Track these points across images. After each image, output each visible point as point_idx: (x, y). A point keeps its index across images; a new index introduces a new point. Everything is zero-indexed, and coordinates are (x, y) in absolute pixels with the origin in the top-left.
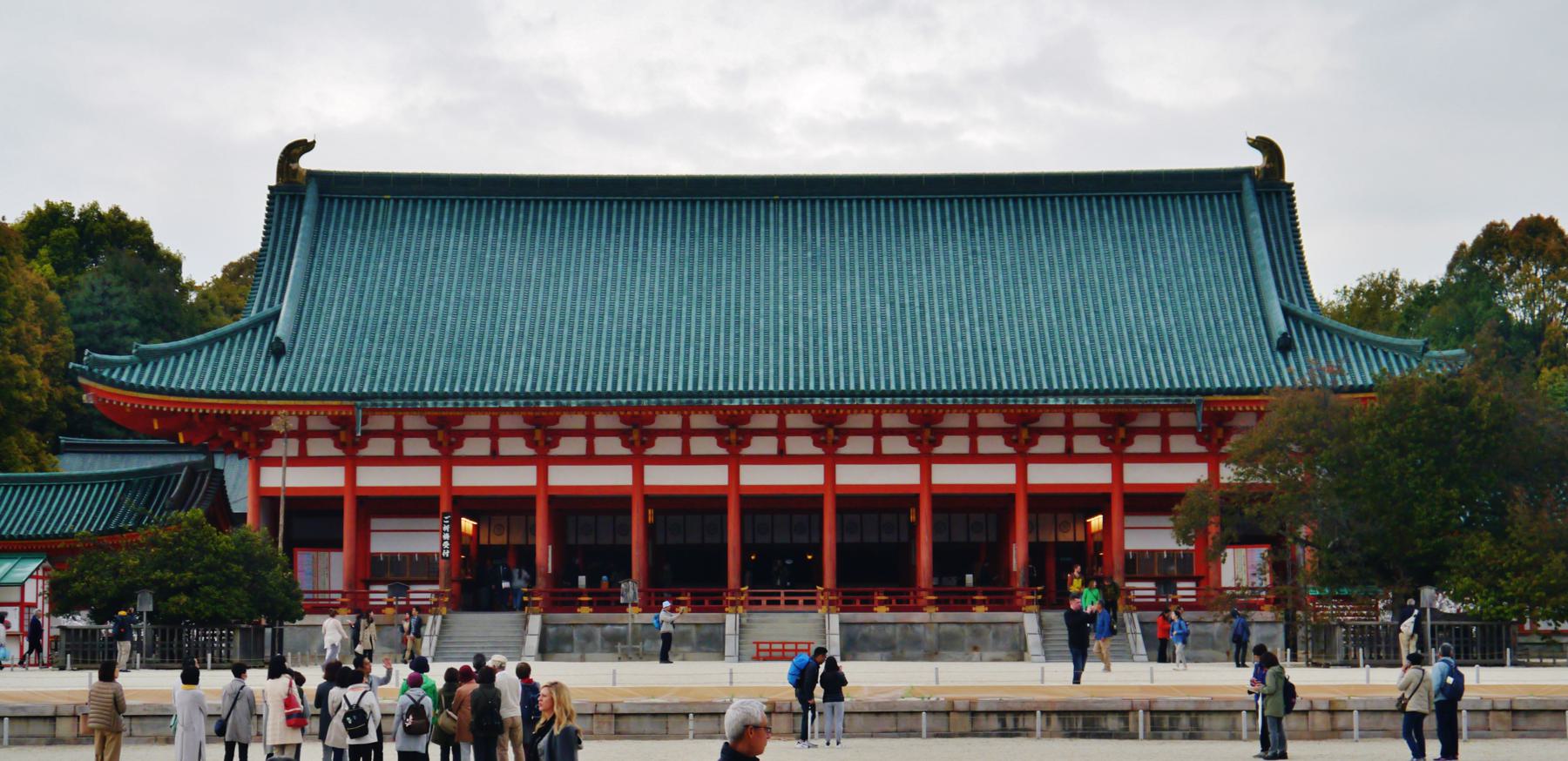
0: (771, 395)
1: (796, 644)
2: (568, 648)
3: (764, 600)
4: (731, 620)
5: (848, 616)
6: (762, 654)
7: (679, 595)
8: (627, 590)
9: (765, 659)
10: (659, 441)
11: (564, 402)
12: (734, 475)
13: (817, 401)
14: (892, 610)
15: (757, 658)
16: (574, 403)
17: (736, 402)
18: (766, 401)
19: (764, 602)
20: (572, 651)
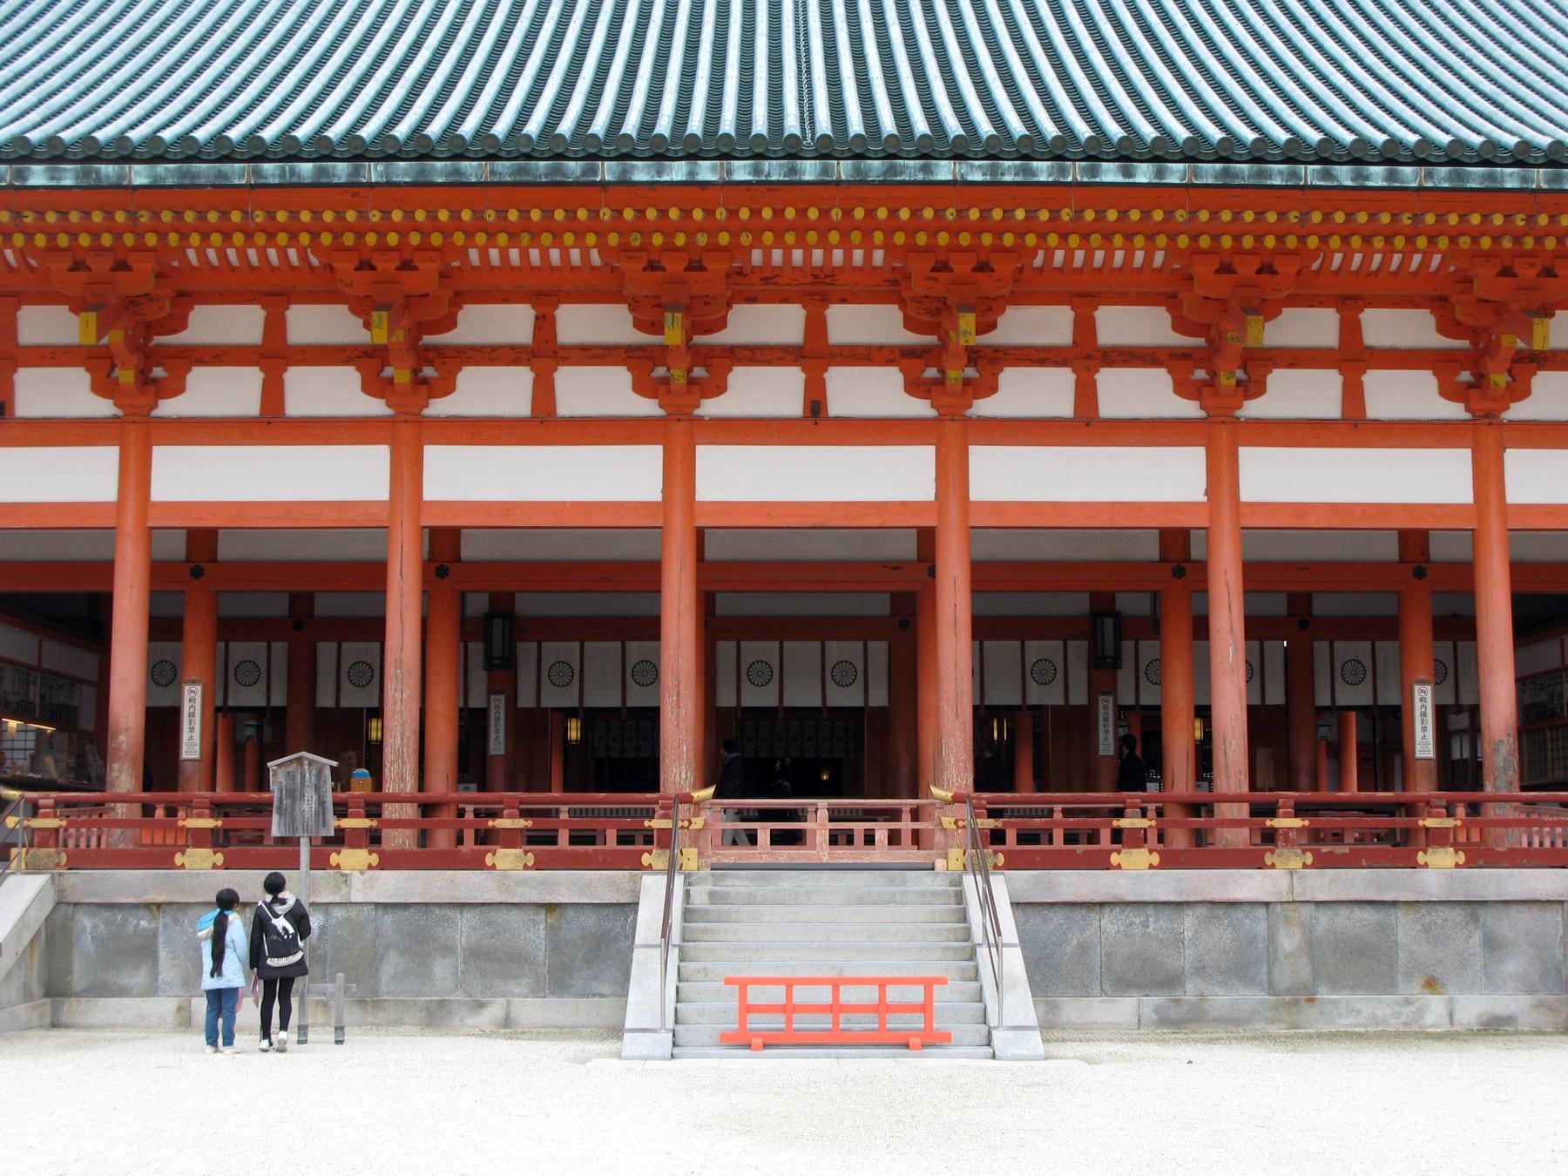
0: (793, 151)
1: (882, 984)
2: (138, 978)
3: (764, 830)
4: (652, 887)
5: (1029, 882)
6: (757, 1022)
7: (494, 814)
8: (294, 794)
9: (770, 1042)
10: (469, 377)
11: (108, 171)
12: (679, 472)
13: (945, 170)
14: (1170, 861)
15: (740, 1041)
16: (140, 175)
17: (677, 171)
18: (774, 170)
19: (764, 836)
20: (152, 990)
